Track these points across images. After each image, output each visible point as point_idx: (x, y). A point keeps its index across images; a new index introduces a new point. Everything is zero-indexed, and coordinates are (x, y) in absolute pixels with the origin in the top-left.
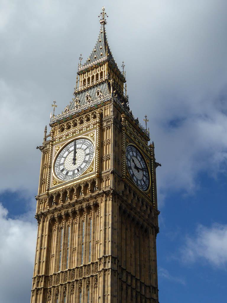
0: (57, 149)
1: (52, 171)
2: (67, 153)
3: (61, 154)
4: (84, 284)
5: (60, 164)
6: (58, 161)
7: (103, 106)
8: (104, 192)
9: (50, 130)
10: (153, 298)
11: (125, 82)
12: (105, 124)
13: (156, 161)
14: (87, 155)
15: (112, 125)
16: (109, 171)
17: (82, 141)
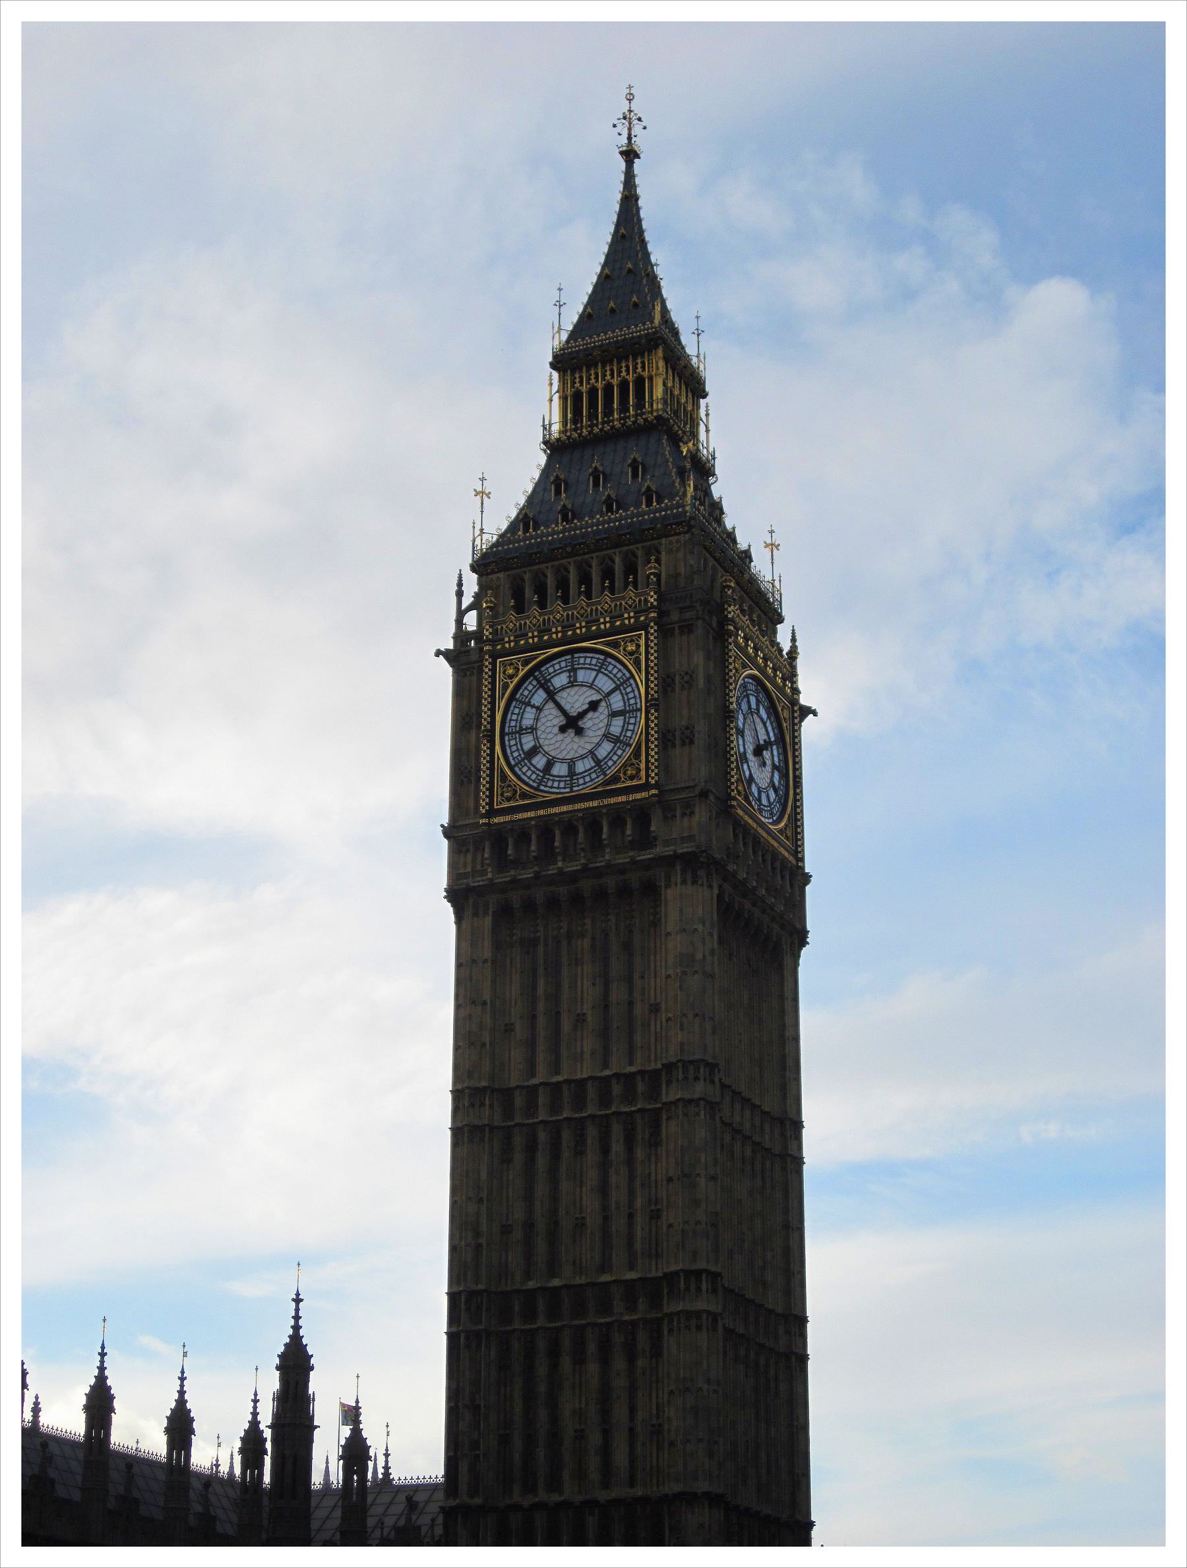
0: (511, 671)
1: (498, 748)
4: (617, 1130)
5: (521, 729)
6: (514, 717)
7: (659, 537)
8: (676, 857)
9: (472, 584)
10: (791, 1156)
11: (705, 396)
12: (675, 616)
13: (804, 700)
14: (614, 714)
15: (700, 622)
16: (694, 787)
17: (594, 661)
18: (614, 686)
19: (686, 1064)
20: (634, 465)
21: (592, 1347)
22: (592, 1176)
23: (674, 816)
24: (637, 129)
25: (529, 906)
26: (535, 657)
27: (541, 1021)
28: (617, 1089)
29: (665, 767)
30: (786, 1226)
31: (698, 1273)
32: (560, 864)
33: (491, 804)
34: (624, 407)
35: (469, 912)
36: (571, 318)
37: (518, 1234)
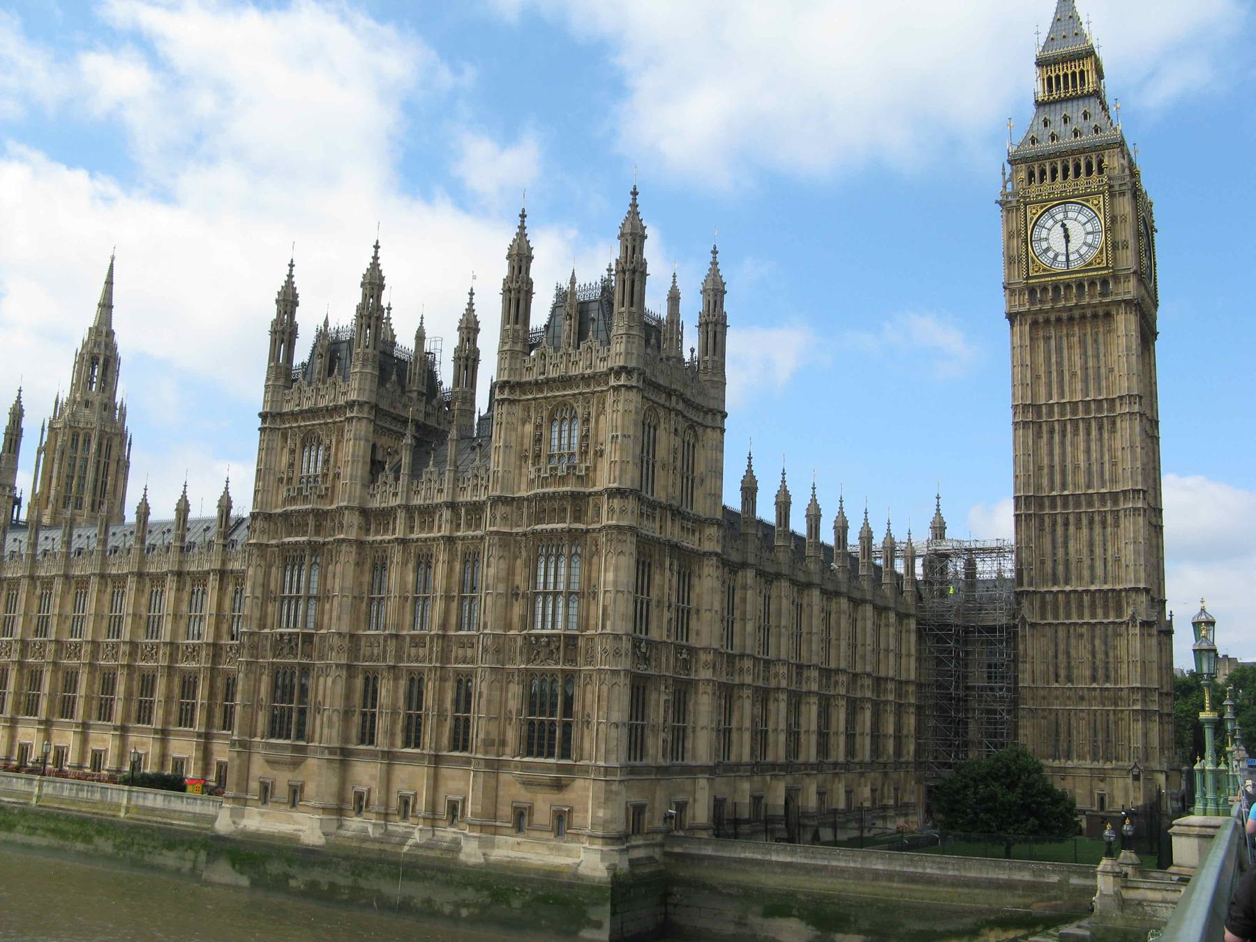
2: (1051, 222)
3: (1041, 222)
9: (1008, 168)
12: (1117, 188)
14: (1088, 233)
19: (1130, 396)
20: (1085, 116)
21: (1085, 521)
22: (1082, 447)
25: (1047, 321)
27: (1054, 374)
28: (1093, 406)
29: (1115, 259)
30: (1154, 468)
31: (1138, 491)
34: (1074, 86)
35: (1017, 323)
36: (1042, 42)
37: (1046, 471)
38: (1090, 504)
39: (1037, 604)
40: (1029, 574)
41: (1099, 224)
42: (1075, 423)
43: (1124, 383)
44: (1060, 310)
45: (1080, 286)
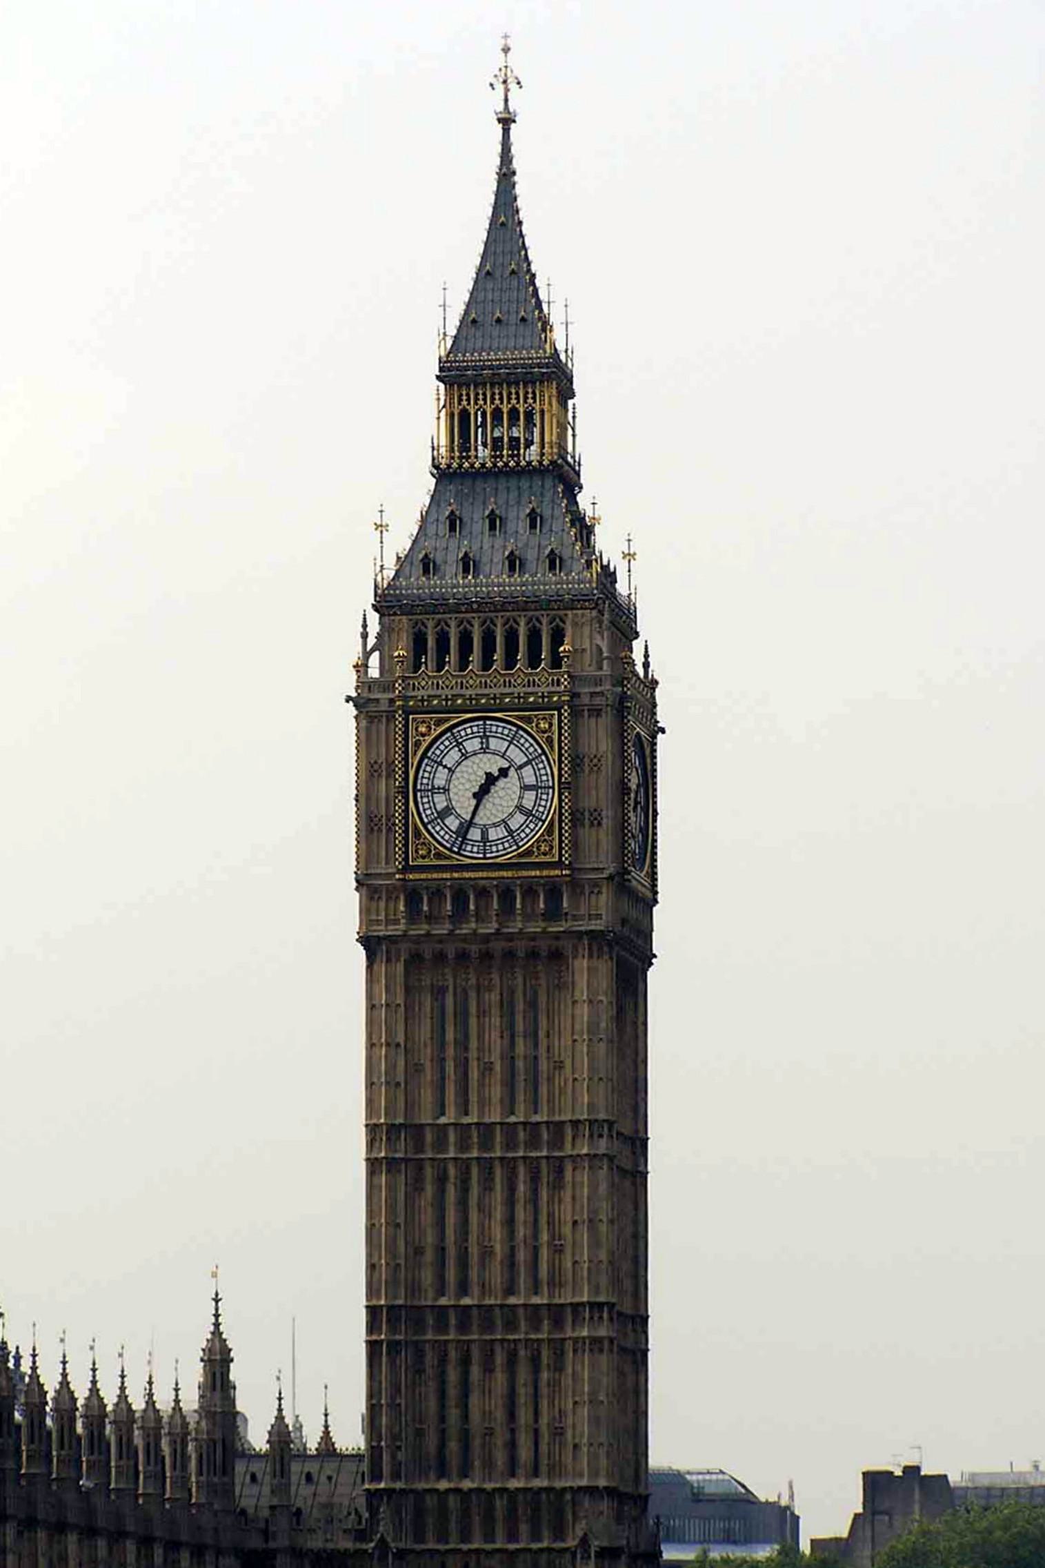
0: (423, 729)
2: (455, 755)
3: (435, 752)
14: (526, 788)
17: (506, 732)
18: (525, 759)
20: (533, 517)
21: (500, 1358)
23: (582, 893)
24: (513, 86)
25: (440, 957)
26: (447, 720)
29: (575, 845)
31: (600, 1305)
32: (473, 925)
33: (406, 859)
35: (381, 956)
37: (429, 1256)
38: (511, 1325)
39: (407, 1517)
40: (393, 1457)
41: (549, 772)
42: (487, 1166)
43: (580, 1098)
44: (464, 938)
45: (507, 896)
